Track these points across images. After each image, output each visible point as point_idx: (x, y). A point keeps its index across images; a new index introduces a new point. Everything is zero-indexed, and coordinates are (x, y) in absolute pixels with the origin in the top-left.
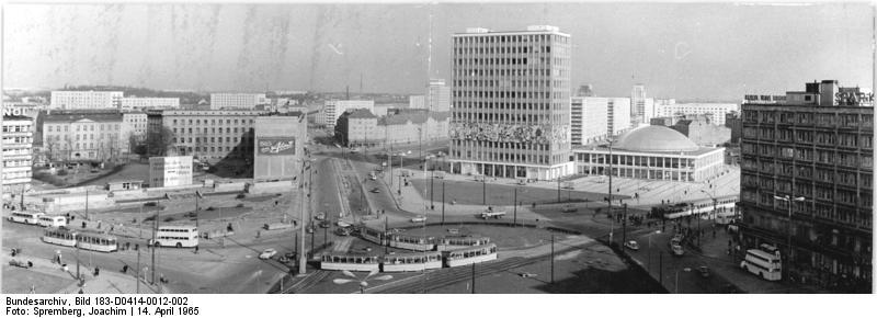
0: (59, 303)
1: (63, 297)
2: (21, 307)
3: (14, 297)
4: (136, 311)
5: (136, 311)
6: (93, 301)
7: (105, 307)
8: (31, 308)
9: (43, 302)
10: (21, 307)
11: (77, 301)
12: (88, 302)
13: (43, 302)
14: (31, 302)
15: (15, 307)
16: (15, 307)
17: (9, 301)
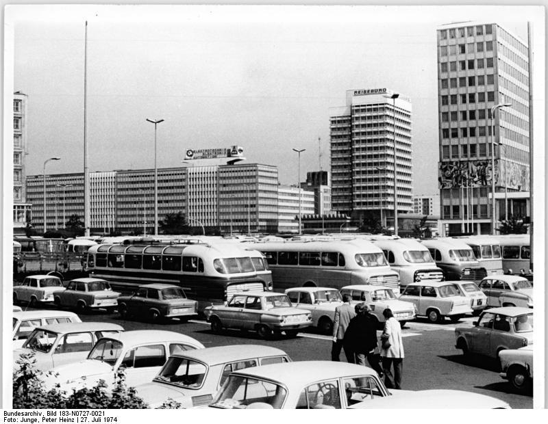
0: (37, 414)
1: (39, 411)
2: (13, 417)
3: (9, 411)
4: (80, 420)
5: (80, 420)
6: (58, 414)
7: (65, 417)
8: (20, 418)
9: (27, 414)
10: (13, 417)
11: (48, 413)
12: (55, 414)
13: (27, 414)
14: (19, 414)
15: (10, 417)
16: (10, 417)
17: (5, 413)
